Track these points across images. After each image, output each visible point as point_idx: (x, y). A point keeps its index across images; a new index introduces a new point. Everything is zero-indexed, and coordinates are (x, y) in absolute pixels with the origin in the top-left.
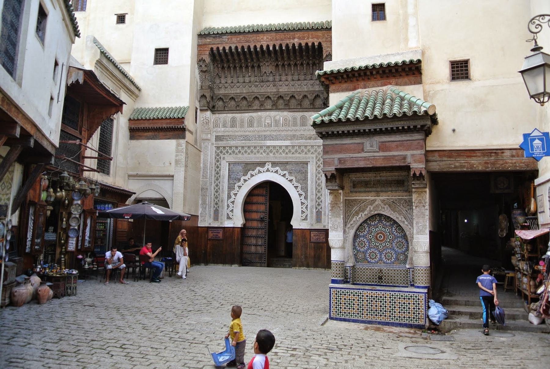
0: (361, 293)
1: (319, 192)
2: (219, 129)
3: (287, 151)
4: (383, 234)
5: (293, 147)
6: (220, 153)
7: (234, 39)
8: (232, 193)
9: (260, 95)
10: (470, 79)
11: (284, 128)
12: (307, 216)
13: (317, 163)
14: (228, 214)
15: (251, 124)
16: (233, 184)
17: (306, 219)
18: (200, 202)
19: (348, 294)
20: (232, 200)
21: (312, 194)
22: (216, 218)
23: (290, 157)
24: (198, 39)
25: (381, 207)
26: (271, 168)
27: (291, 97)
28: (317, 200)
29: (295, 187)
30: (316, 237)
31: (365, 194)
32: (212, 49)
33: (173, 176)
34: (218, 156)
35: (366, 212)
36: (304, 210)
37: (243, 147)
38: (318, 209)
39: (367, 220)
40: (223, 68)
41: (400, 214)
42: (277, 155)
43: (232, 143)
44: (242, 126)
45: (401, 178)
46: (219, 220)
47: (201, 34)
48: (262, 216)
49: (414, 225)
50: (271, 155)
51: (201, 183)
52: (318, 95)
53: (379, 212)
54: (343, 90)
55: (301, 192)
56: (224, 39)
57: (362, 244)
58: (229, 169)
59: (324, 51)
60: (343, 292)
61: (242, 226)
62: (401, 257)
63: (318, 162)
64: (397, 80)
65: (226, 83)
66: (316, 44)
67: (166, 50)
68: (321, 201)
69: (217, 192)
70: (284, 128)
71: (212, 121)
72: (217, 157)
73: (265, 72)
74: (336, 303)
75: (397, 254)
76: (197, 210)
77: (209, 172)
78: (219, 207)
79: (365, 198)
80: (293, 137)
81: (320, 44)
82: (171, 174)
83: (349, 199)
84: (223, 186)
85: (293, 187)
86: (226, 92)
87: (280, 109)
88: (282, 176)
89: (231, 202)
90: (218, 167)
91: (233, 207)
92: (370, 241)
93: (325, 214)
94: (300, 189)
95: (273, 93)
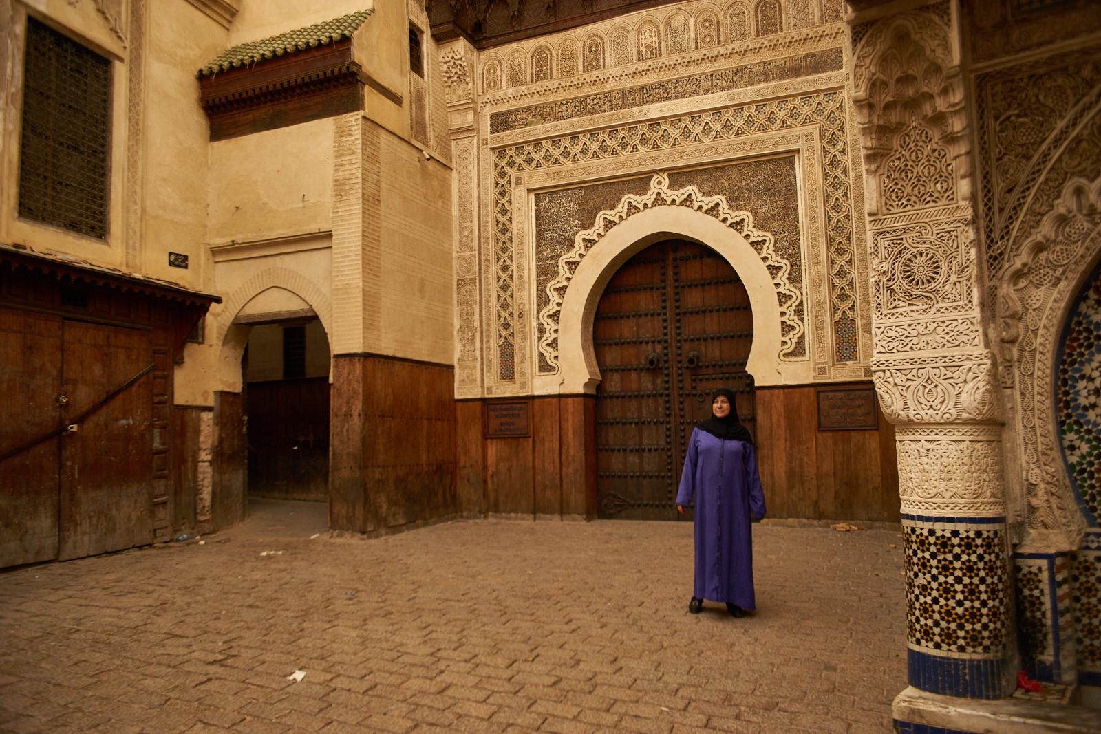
1: (840, 251)
2: (501, 93)
5: (738, 108)
6: (507, 168)
12: (801, 339)
13: (825, 152)
14: (541, 355)
15: (594, 58)
16: (552, 258)
17: (799, 351)
18: (457, 323)
20: (551, 308)
21: (817, 263)
22: (507, 373)
23: (728, 149)
28: (836, 280)
29: (752, 243)
33: (328, 236)
36: (791, 319)
37: (574, 136)
38: (839, 313)
42: (686, 145)
44: (567, 70)
46: (516, 376)
50: (666, 148)
51: (456, 264)
55: (776, 260)
58: (538, 212)
63: (829, 148)
68: (851, 285)
69: (505, 287)
70: (701, 53)
72: (501, 181)
76: (448, 350)
80: (737, 77)
82: (325, 227)
85: (746, 243)
88: (707, 212)
89: (549, 316)
91: (556, 331)
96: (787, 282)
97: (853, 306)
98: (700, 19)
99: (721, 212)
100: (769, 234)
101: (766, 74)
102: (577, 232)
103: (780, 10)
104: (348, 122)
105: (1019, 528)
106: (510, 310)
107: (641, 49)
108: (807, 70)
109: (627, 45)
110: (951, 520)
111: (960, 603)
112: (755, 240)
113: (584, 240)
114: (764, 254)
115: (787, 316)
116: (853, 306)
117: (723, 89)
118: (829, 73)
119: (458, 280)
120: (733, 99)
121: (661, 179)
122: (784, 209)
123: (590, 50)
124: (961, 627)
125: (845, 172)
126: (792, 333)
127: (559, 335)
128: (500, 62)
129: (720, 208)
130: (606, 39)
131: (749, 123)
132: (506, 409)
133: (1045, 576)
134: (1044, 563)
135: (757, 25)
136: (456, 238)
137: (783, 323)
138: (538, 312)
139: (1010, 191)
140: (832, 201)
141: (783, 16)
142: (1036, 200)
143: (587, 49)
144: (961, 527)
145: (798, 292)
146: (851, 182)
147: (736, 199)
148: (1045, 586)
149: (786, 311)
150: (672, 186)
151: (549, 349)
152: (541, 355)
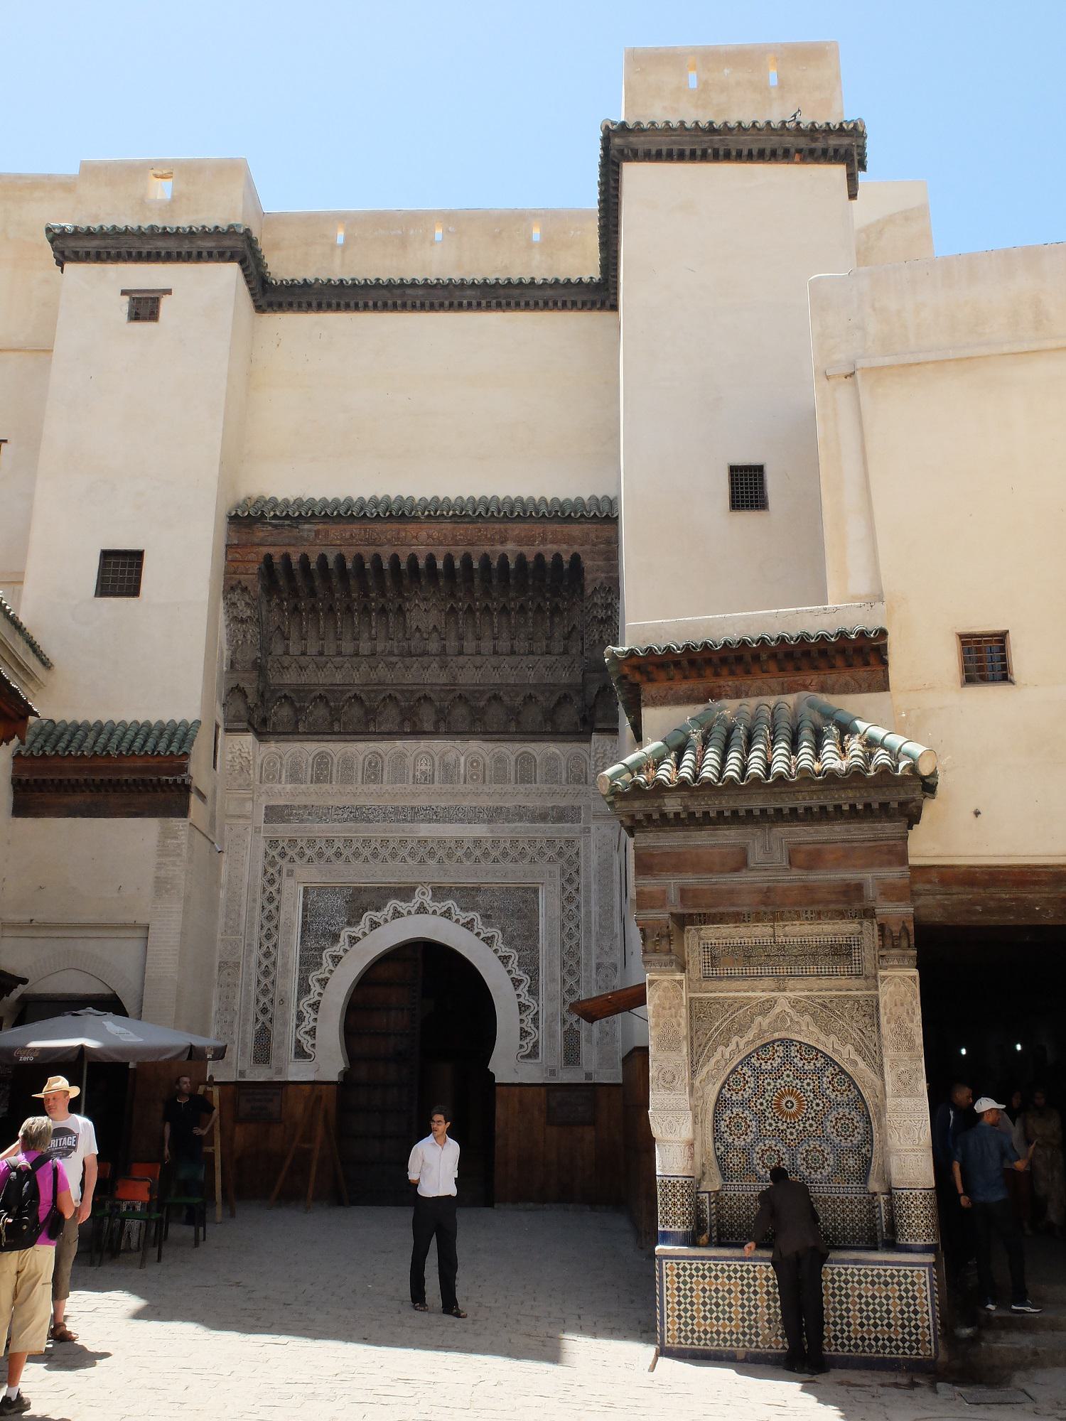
0: (748, 1271)
1: (571, 973)
2: (279, 786)
4: (797, 1097)
6: (277, 859)
7: (335, 531)
8: (313, 977)
9: (402, 692)
10: (1012, 682)
11: (469, 786)
12: (535, 1045)
13: (564, 889)
14: (298, 1041)
16: (316, 949)
17: (533, 1054)
18: (215, 1006)
19: (713, 1274)
20: (312, 997)
21: (553, 980)
24: (229, 530)
25: (792, 1020)
26: (430, 902)
27: (489, 700)
28: (567, 997)
29: (500, 957)
31: (746, 984)
32: (269, 558)
35: (750, 1035)
36: (528, 1026)
39: (749, 1056)
40: (296, 610)
41: (844, 1041)
43: (319, 829)
45: (841, 940)
46: (273, 1062)
47: (236, 515)
49: (887, 1068)
52: (565, 696)
53: (783, 1035)
54: (679, 701)
55: (518, 974)
56: (305, 534)
57: (738, 1126)
59: (588, 577)
60: (697, 1269)
62: (851, 1162)
64: (822, 678)
65: (304, 654)
66: (566, 558)
67: (136, 558)
69: (266, 973)
71: (259, 761)
72: (271, 870)
73: (418, 629)
74: (679, 1303)
75: (840, 1154)
77: (243, 913)
79: (747, 994)
80: (494, 815)
81: (576, 558)
82: (142, 920)
83: (701, 999)
85: (495, 957)
86: (303, 680)
89: (310, 1005)
90: (271, 899)
92: (761, 1117)
93: (589, 1041)
94: (515, 965)
95: (438, 688)
96: (526, 993)
98: (469, 759)
101: (520, 814)
103: (535, 765)
104: (176, 826)
105: (699, 1182)
107: (417, 773)
109: (404, 768)
110: (677, 1176)
111: (679, 1209)
113: (350, 937)
114: (509, 968)
115: (526, 1023)
117: (484, 822)
118: (568, 825)
120: (492, 831)
121: (425, 890)
122: (528, 931)
123: (370, 763)
124: (679, 1218)
125: (577, 907)
126: (528, 1038)
127: (318, 1024)
128: (280, 757)
129: (475, 923)
130: (386, 759)
131: (505, 854)
133: (707, 1200)
134: (707, 1195)
136: (221, 921)
137: (521, 1029)
138: (298, 1000)
139: (700, 1046)
142: (708, 1051)
143: (366, 763)
144: (680, 1179)
145: (536, 1005)
147: (489, 917)
148: (707, 1204)
149: (525, 1019)
152: (298, 1041)
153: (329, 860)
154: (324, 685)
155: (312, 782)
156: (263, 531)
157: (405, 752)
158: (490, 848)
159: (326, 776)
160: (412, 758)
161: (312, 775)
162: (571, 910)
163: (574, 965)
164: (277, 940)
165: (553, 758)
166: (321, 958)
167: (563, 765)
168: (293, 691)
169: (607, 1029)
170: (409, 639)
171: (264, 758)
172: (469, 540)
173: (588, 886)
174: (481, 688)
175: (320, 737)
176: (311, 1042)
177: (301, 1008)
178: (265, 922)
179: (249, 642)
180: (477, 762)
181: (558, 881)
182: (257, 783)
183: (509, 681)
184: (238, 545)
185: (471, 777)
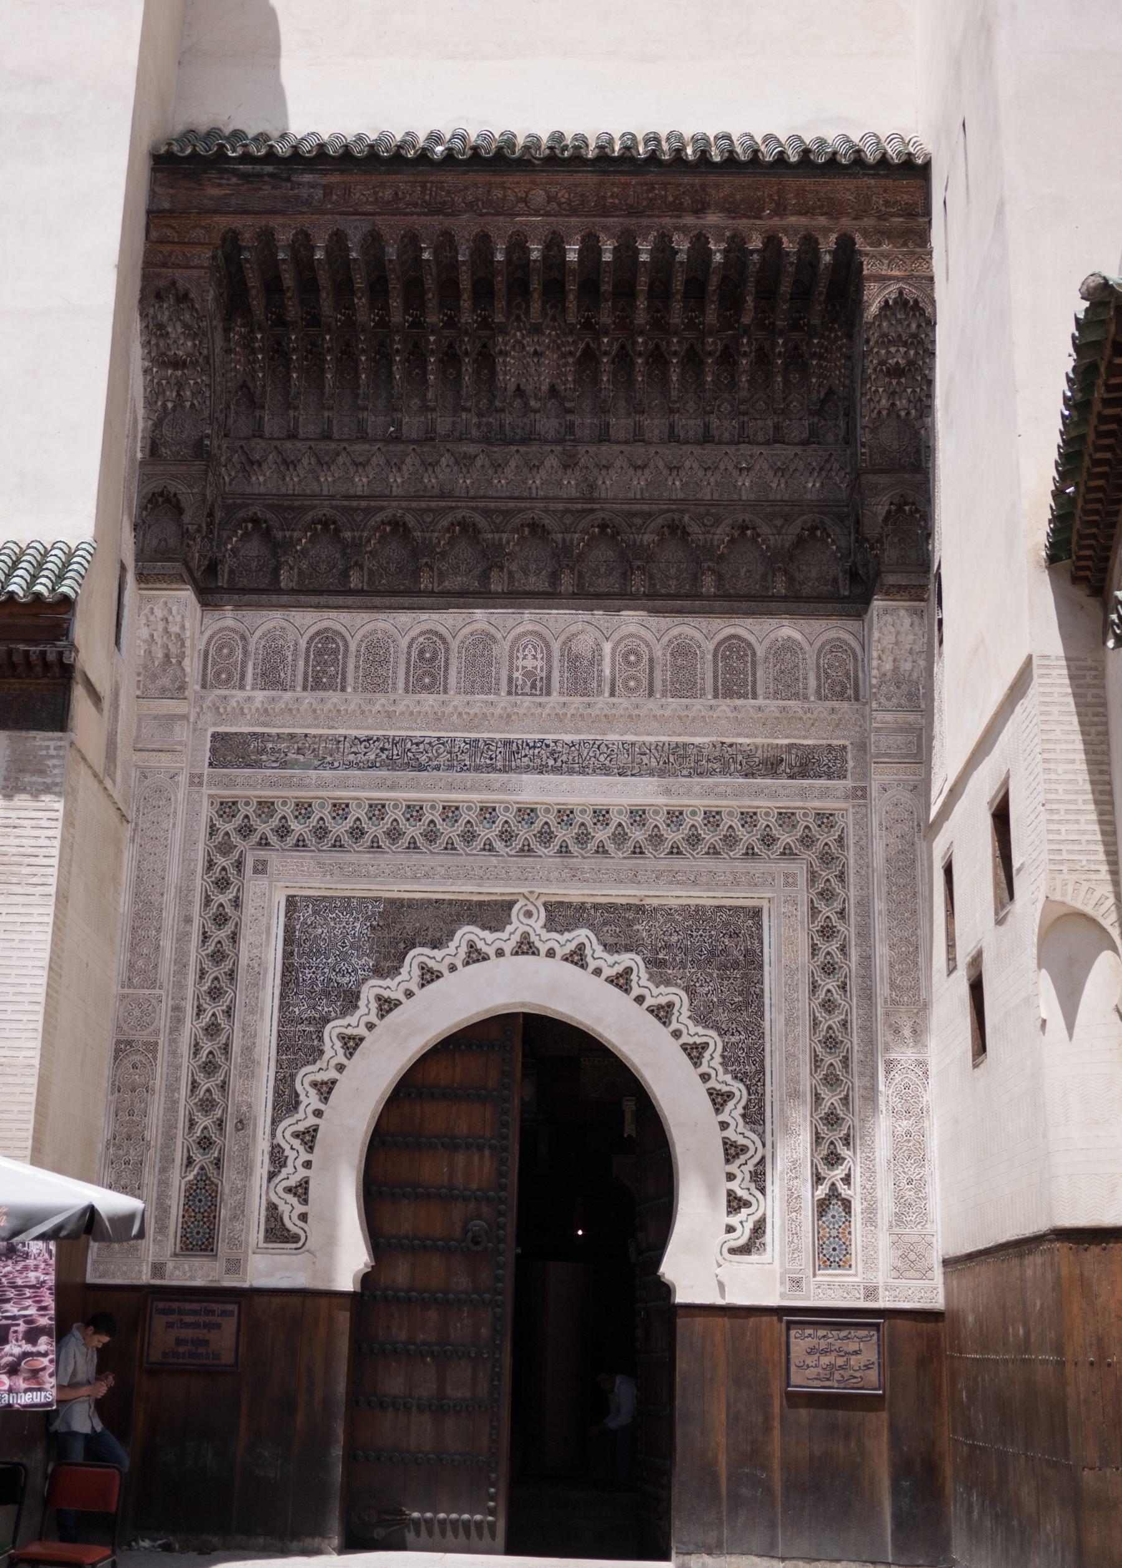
1: (832, 1081)
2: (239, 695)
3: (638, 835)
6: (235, 839)
8: (305, 1078)
9: (487, 513)
11: (621, 701)
13: (814, 911)
14: (272, 1207)
16: (310, 1021)
20: (303, 1119)
24: (154, 181)
30: (825, 1360)
34: (224, 854)
40: (279, 352)
46: (222, 1248)
48: (478, 1224)
55: (724, 1081)
56: (304, 192)
58: (289, 931)
61: (359, 1290)
72: (221, 861)
73: (519, 391)
78: (218, 1163)
84: (251, 1034)
85: (675, 1046)
87: (598, 596)
89: (296, 1135)
90: (221, 919)
95: (560, 506)
97: (848, 1176)
99: (634, 984)
100: (714, 1033)
102: (365, 980)
103: (754, 663)
106: (218, 1113)
107: (516, 675)
108: (791, 767)
112: (691, 1041)
113: (379, 998)
114: (704, 1068)
115: (737, 1181)
116: (848, 1176)
117: (651, 774)
119: (118, 1042)
121: (531, 908)
123: (422, 652)
125: (843, 949)
128: (243, 638)
129: (634, 977)
130: (454, 644)
132: (194, 1312)
135: (715, 678)
138: (275, 1122)
140: (821, 994)
141: (760, 673)
143: (414, 654)
145: (759, 1144)
146: (853, 966)
149: (737, 1172)
150: (551, 924)
151: (290, 1198)
152: (272, 1207)
153: (338, 845)
154: (332, 497)
155: (305, 688)
156: (220, 185)
157: (493, 631)
158: (663, 826)
159: (333, 677)
160: (506, 645)
161: (306, 674)
162: (828, 953)
163: (838, 1066)
164: (233, 1000)
165: (788, 647)
166: (321, 1039)
167: (811, 661)
168: (268, 507)
169: (910, 1195)
170: (502, 410)
171: (211, 637)
172: (631, 207)
173: (865, 905)
174: (646, 508)
175: (322, 599)
176: (300, 1209)
177: (279, 1139)
178: (208, 965)
179: (188, 404)
180: (636, 653)
181: (803, 894)
182: (197, 687)
183: (699, 496)
184: (171, 211)
185: (625, 683)
